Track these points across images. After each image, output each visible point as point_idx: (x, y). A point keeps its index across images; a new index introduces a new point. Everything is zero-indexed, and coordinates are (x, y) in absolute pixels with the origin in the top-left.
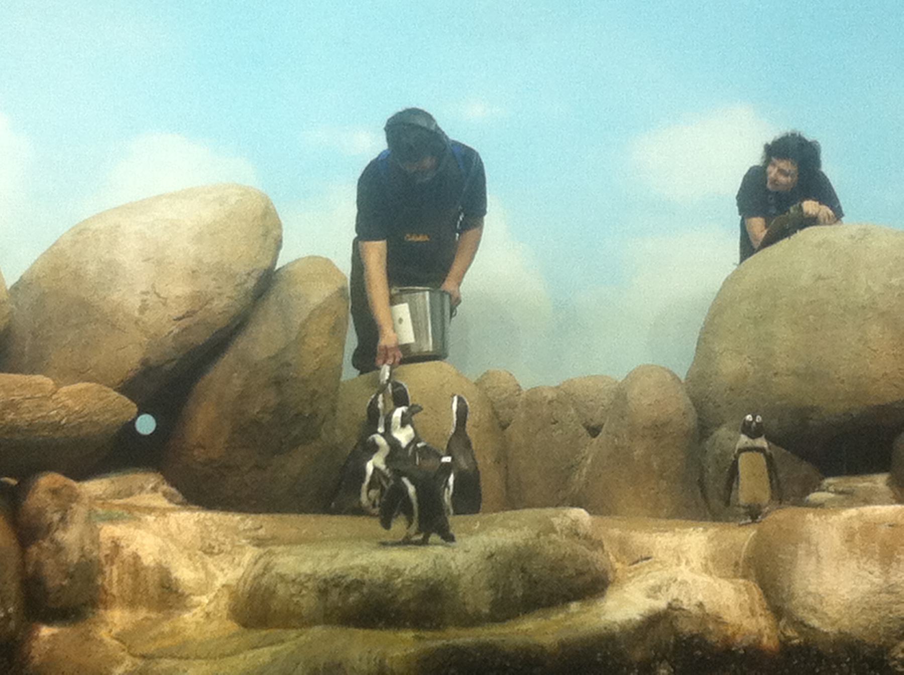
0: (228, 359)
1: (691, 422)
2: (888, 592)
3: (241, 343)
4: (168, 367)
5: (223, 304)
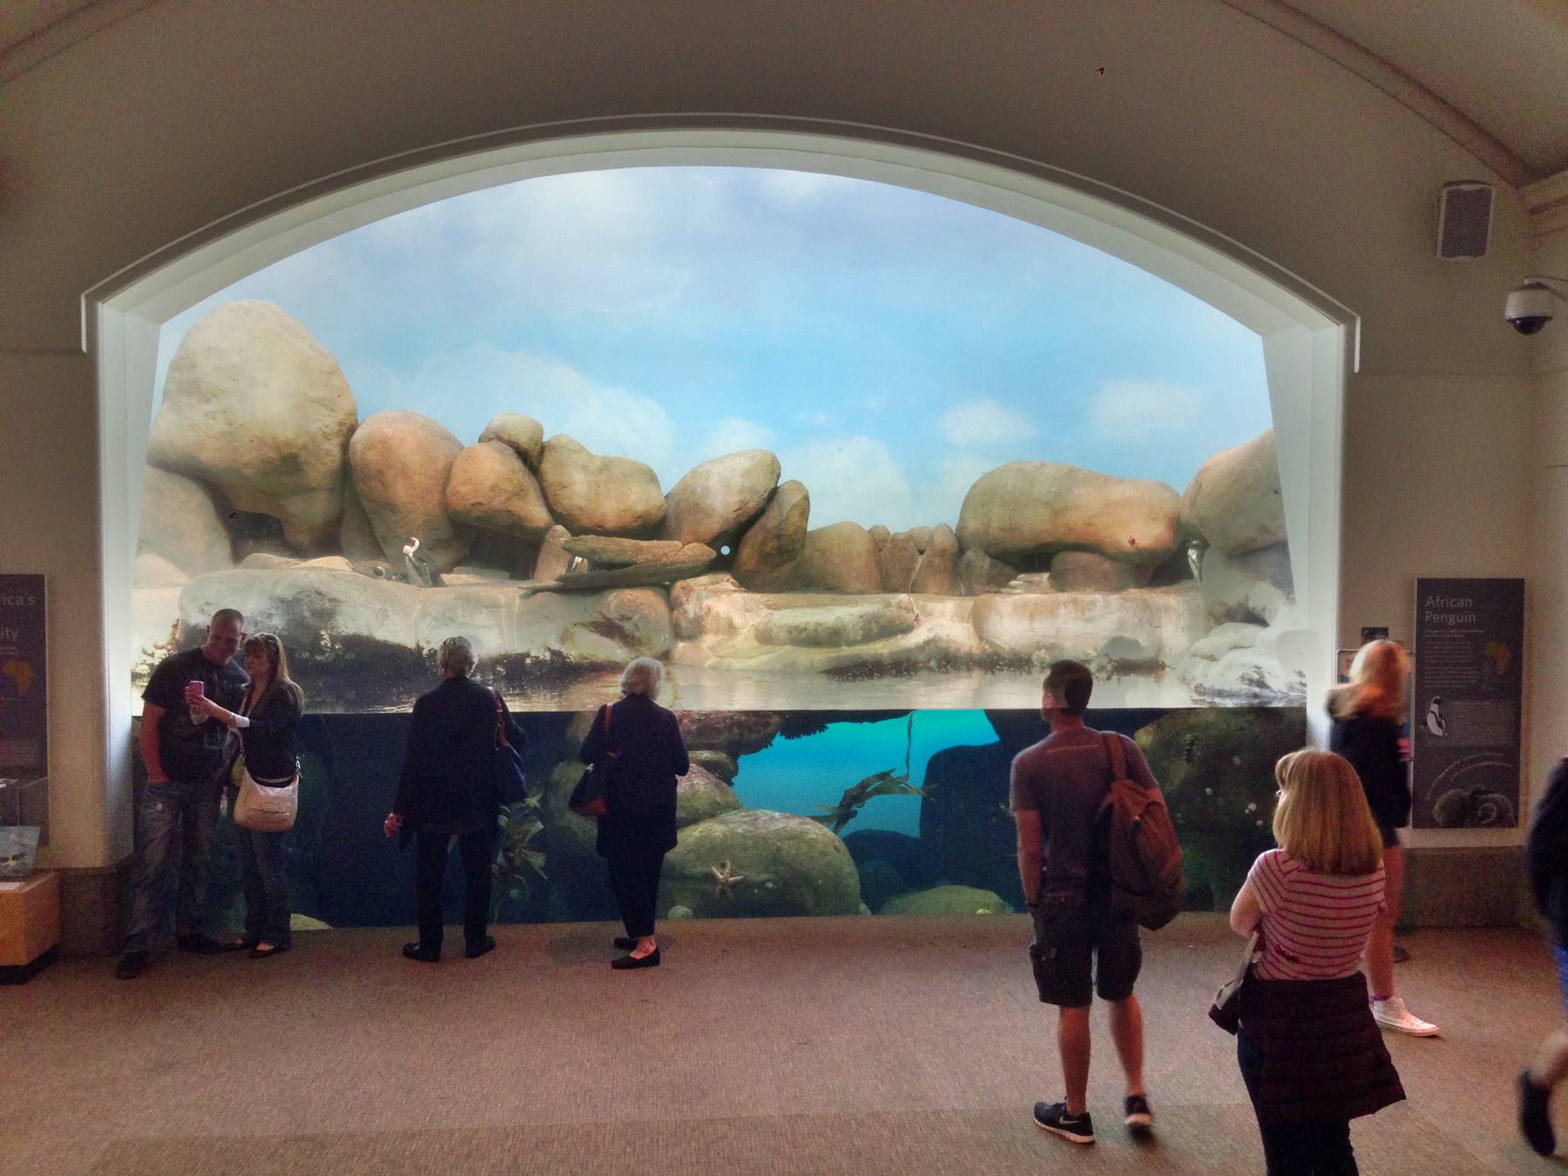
0: (757, 527)
1: (956, 549)
3: (762, 520)
5: (753, 503)
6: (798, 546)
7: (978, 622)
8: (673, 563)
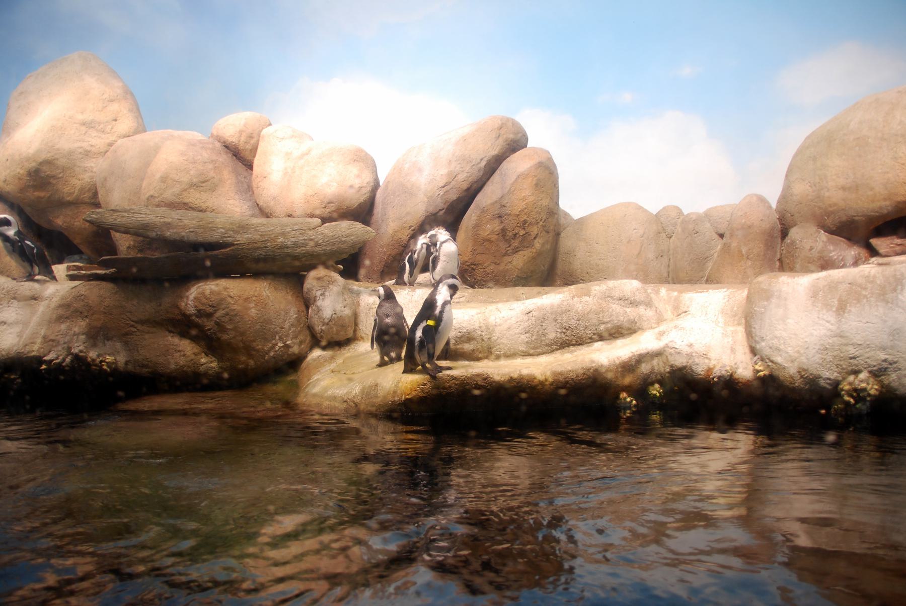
2: (841, 336)
4: (441, 213)
5: (465, 176)
6: (534, 230)
7: (749, 319)
8: (296, 245)
